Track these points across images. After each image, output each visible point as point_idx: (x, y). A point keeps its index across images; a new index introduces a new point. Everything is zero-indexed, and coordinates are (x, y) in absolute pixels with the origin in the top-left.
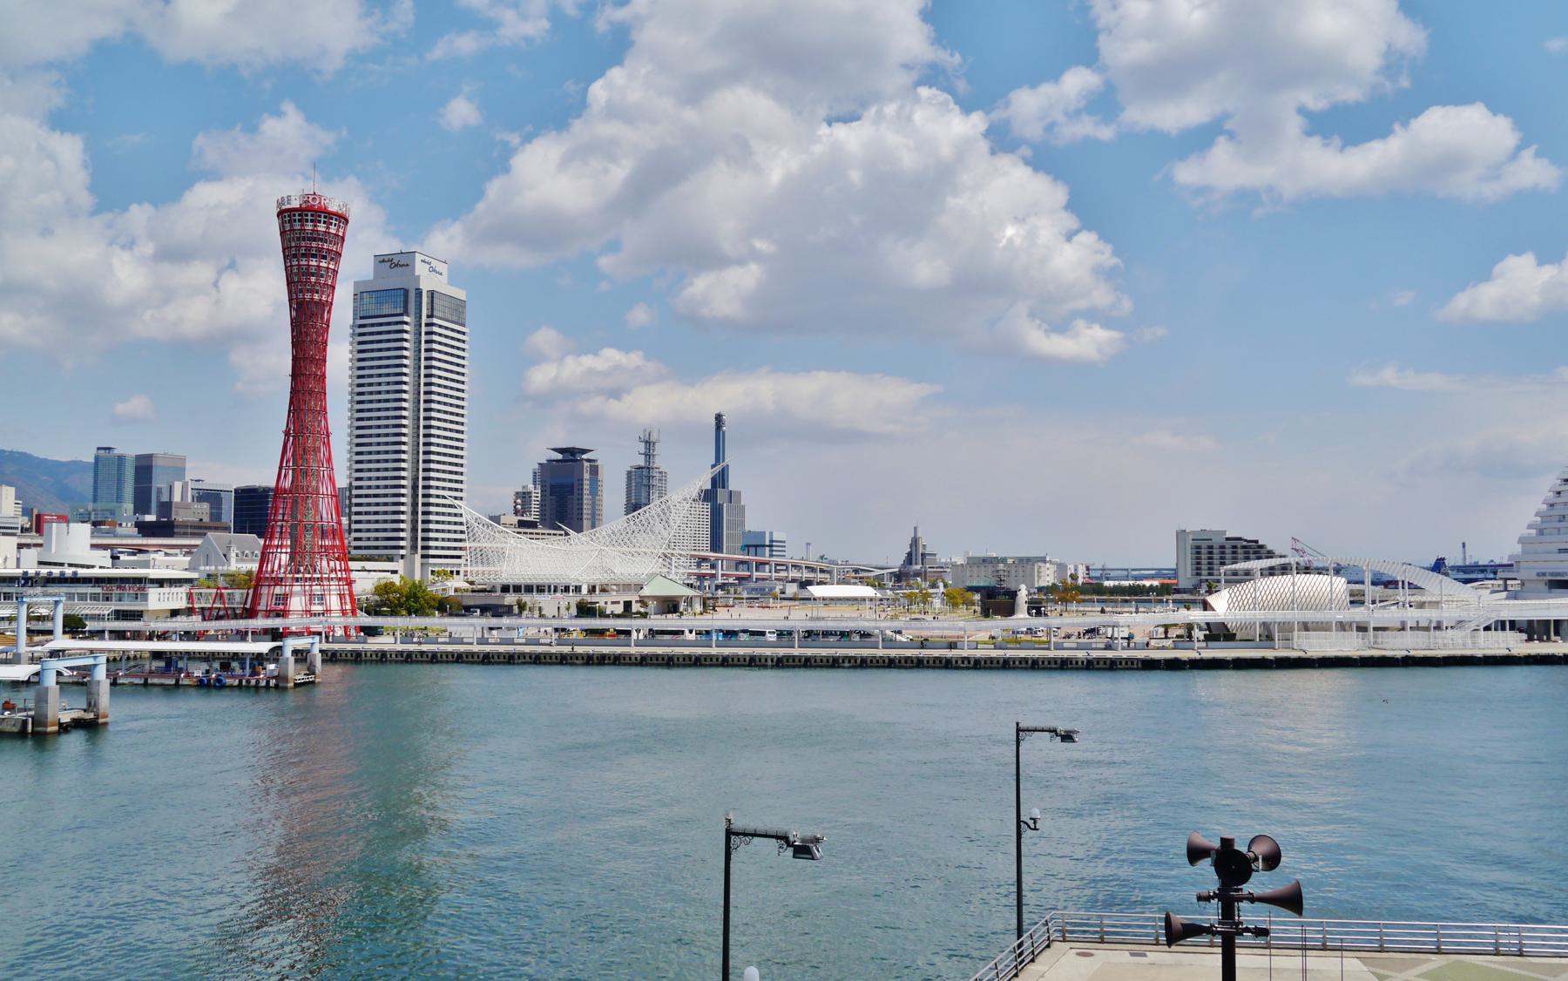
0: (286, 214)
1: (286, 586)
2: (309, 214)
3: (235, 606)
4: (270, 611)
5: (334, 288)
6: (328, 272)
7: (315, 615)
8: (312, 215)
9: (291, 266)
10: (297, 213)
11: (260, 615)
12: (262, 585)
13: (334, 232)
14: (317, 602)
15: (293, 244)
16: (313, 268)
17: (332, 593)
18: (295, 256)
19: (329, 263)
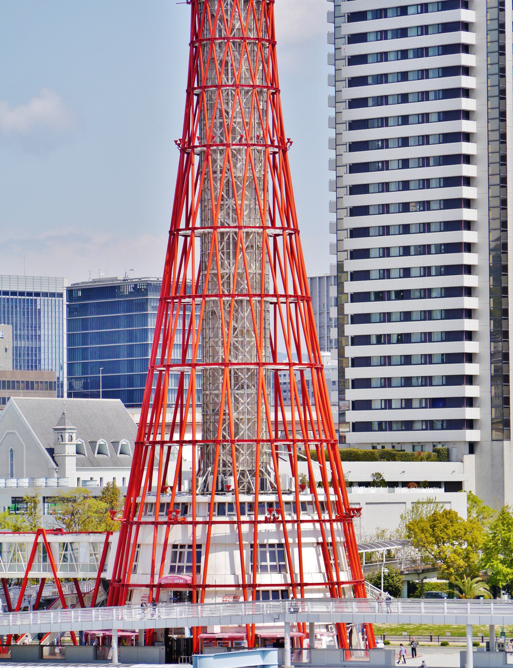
1: (195, 523)
3: (80, 575)
4: (160, 586)
7: (266, 595)
11: (138, 595)
12: (139, 524)
14: (269, 563)
17: (304, 540)
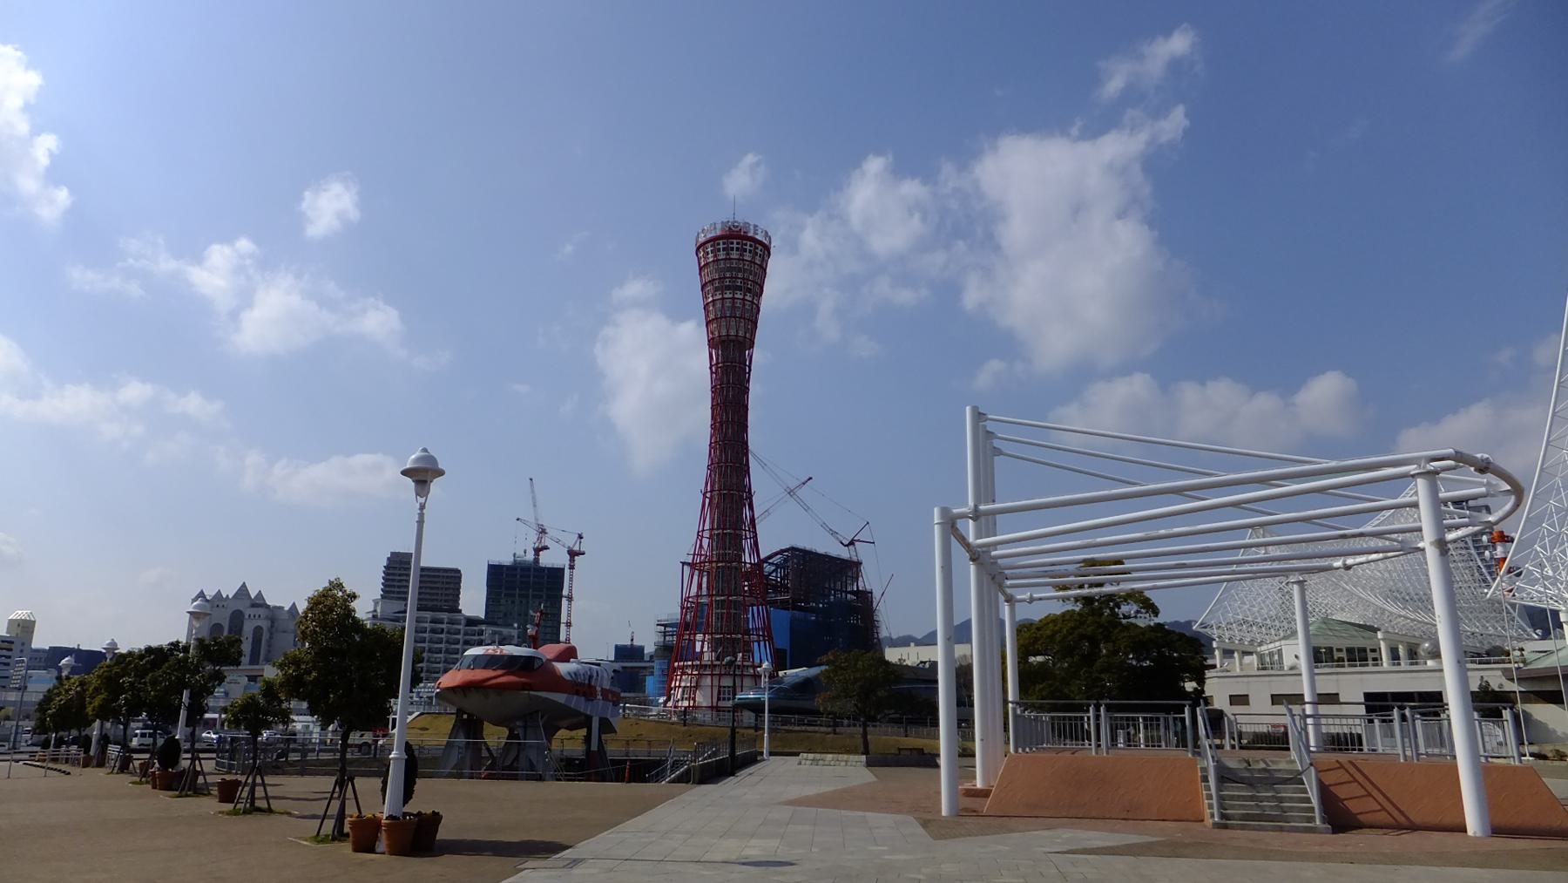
2: (735, 241)
5: (755, 323)
6: (744, 305)
10: (721, 242)
16: (739, 301)
19: (745, 295)
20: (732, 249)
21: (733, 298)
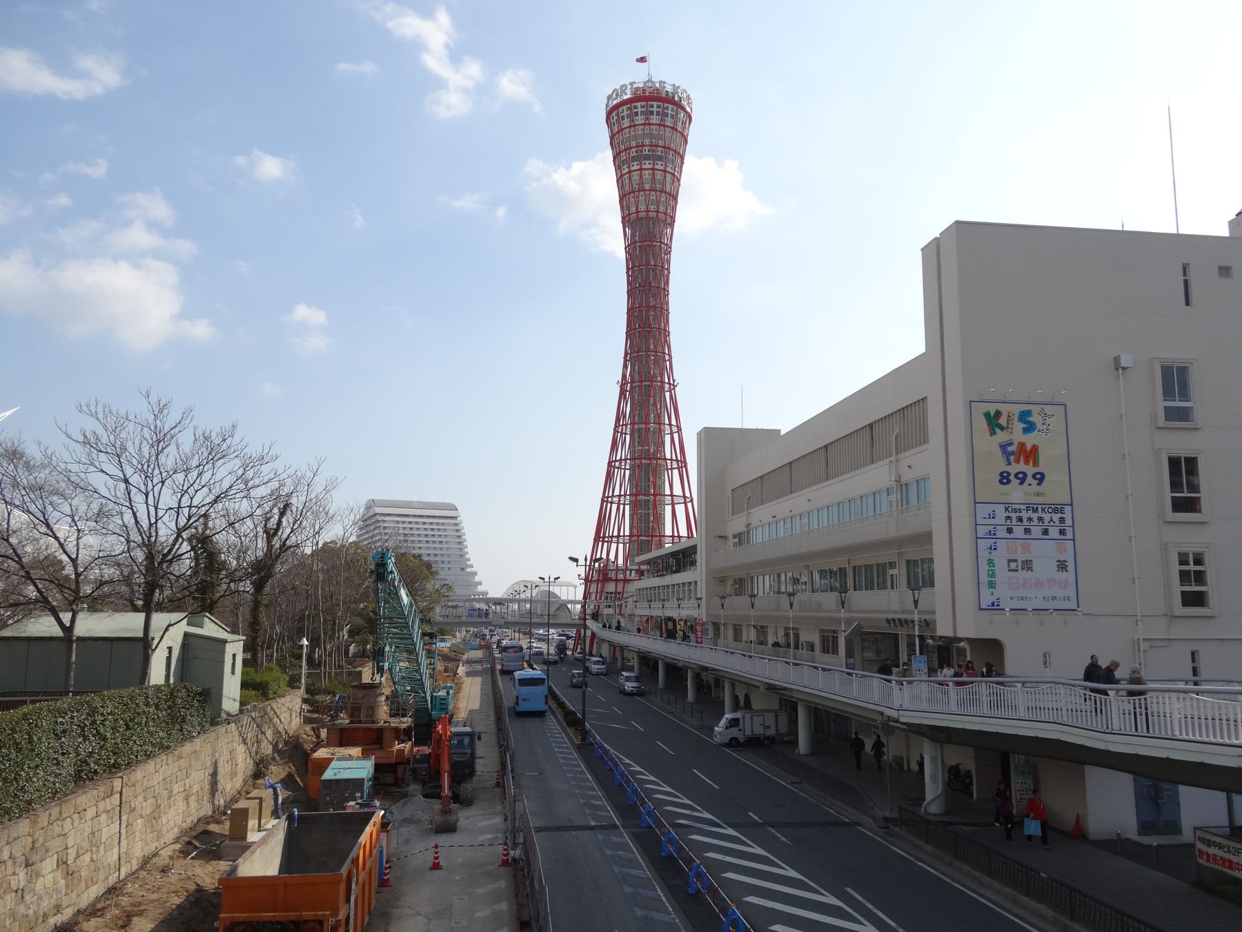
0: (625, 107)
2: (655, 104)
8: (658, 107)
9: (630, 172)
13: (670, 125)
15: (623, 147)
16: (659, 172)
18: (634, 159)
20: (652, 113)
21: (653, 169)
